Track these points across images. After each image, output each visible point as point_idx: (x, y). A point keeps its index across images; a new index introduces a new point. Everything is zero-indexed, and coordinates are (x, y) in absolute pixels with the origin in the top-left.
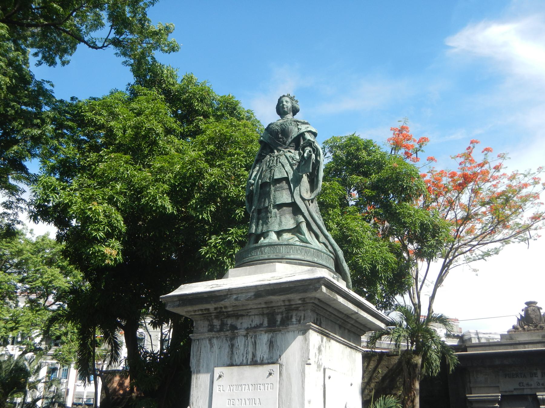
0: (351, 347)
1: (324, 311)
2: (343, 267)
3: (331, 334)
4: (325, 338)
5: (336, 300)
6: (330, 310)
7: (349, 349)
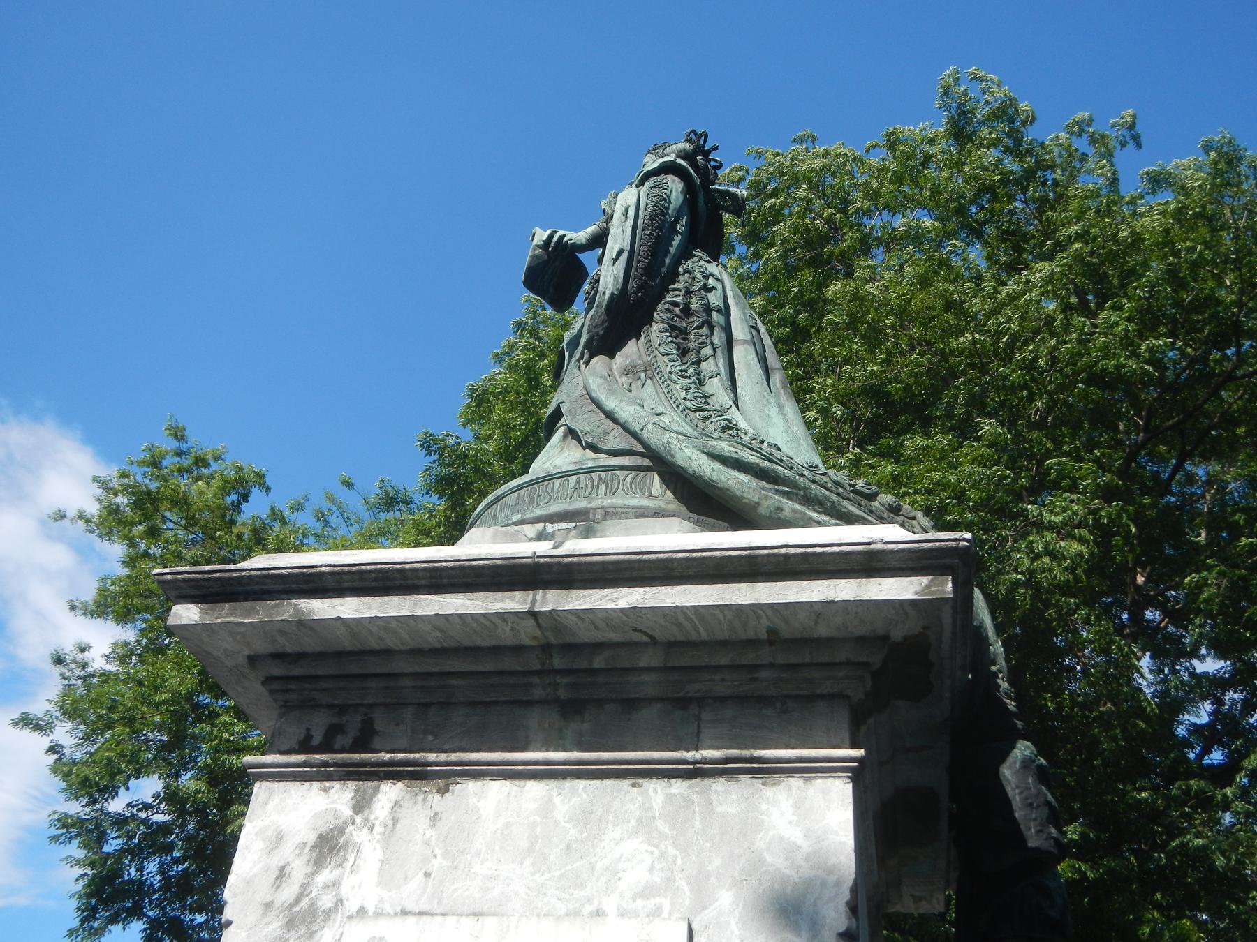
0: (694, 772)
1: (372, 684)
2: (684, 470)
3: (432, 757)
4: (390, 791)
5: (306, 624)
6: (404, 666)
7: (657, 791)
